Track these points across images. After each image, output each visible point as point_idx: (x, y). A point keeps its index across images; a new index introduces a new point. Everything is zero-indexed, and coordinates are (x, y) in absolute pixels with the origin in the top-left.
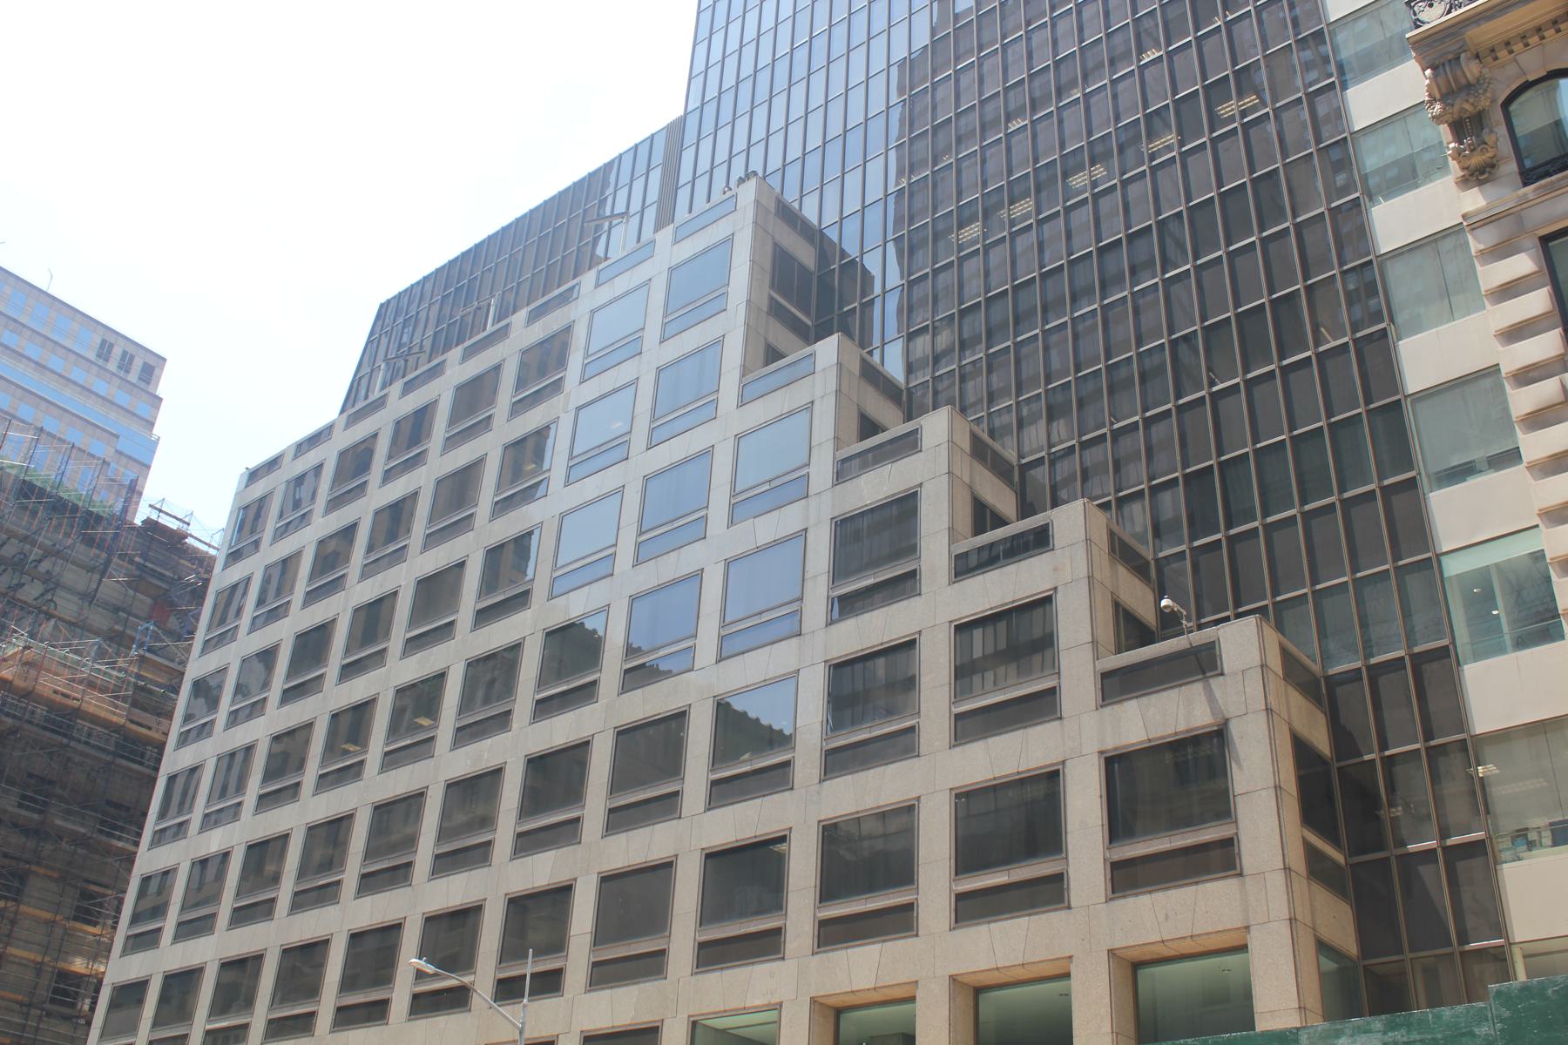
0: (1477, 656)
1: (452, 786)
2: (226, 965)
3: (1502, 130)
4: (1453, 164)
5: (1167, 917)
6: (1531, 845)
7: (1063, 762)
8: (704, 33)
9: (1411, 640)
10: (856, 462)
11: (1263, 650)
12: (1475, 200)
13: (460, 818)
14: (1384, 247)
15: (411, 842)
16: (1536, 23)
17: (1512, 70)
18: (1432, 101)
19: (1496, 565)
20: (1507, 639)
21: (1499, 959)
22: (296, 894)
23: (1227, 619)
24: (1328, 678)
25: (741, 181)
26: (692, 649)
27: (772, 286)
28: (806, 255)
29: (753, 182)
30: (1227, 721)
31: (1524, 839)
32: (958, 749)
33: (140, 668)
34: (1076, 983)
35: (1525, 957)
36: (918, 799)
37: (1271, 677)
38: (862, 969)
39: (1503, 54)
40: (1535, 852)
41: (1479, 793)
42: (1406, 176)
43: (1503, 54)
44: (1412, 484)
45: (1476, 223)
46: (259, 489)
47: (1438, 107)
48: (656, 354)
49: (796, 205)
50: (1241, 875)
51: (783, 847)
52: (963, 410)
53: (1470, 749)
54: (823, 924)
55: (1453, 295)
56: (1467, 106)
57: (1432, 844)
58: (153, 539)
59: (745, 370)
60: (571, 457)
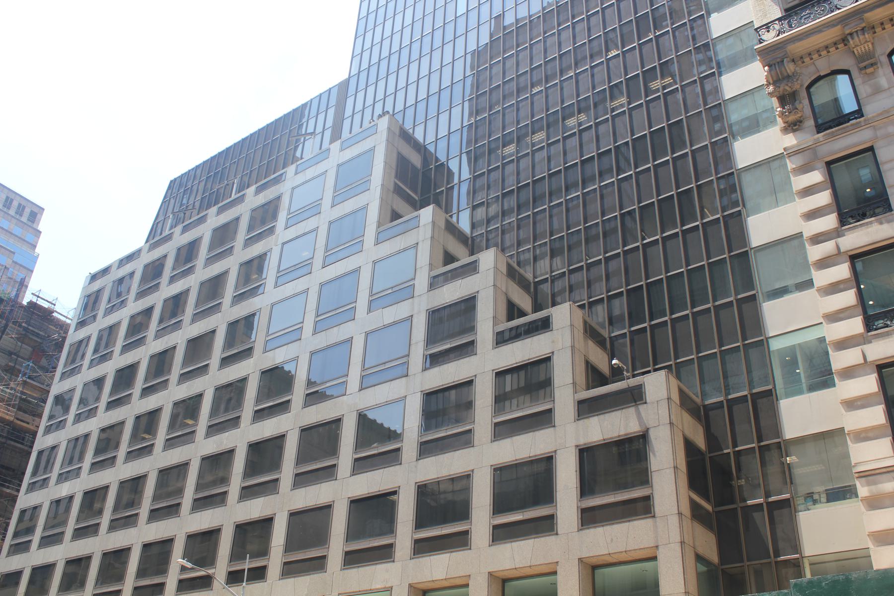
0: (787, 395)
1: (204, 459)
2: (70, 562)
3: (806, 102)
4: (779, 120)
5: (612, 540)
6: (815, 502)
7: (555, 451)
8: (361, 31)
9: (751, 385)
10: (441, 278)
11: (669, 390)
12: (791, 140)
13: (209, 478)
14: (741, 165)
15: (180, 492)
16: (825, 43)
17: (812, 69)
18: (768, 84)
19: (799, 344)
20: (804, 386)
21: (797, 565)
22: (112, 521)
23: (649, 372)
24: (705, 406)
25: (380, 116)
26: (345, 382)
27: (396, 177)
28: (416, 160)
29: (387, 117)
30: (648, 430)
31: (811, 498)
33: (23, 388)
34: (560, 579)
35: (810, 564)
36: (473, 471)
37: (673, 405)
38: (438, 567)
39: (807, 60)
40: (817, 506)
41: (787, 472)
42: (753, 126)
43: (807, 60)
44: (753, 298)
45: (791, 153)
46: (97, 285)
47: (771, 88)
48: (329, 213)
49: (411, 131)
50: (654, 516)
51: (395, 497)
53: (783, 447)
54: (417, 542)
55: (778, 193)
56: (787, 88)
57: (761, 500)
58: (33, 313)
59: (379, 224)
60: (278, 272)
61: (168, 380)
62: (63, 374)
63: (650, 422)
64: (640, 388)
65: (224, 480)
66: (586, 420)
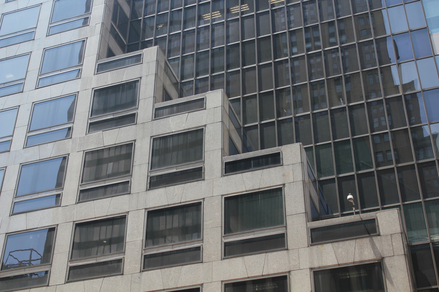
7: (289, 272)
10: (167, 110)
23: (378, 209)
28: (127, 10)
30: (383, 259)
32: (226, 260)
36: (202, 285)
52: (228, 95)
63: (385, 253)
64: (373, 221)
66: (319, 246)
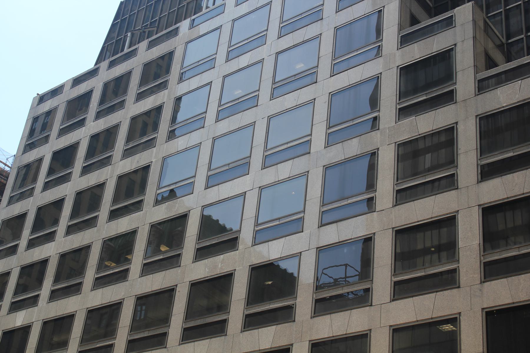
1: (195, 285)
10: (493, 80)
13: (204, 303)
15: (166, 320)
46: (47, 106)
60: (274, 83)
61: (141, 201)
62: (11, 198)
65: (223, 307)
